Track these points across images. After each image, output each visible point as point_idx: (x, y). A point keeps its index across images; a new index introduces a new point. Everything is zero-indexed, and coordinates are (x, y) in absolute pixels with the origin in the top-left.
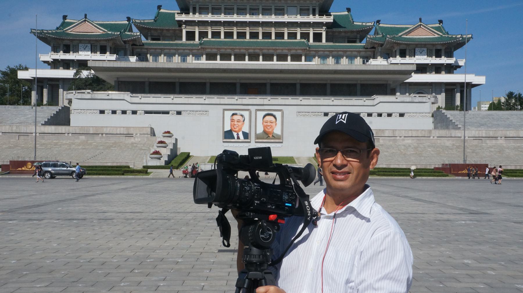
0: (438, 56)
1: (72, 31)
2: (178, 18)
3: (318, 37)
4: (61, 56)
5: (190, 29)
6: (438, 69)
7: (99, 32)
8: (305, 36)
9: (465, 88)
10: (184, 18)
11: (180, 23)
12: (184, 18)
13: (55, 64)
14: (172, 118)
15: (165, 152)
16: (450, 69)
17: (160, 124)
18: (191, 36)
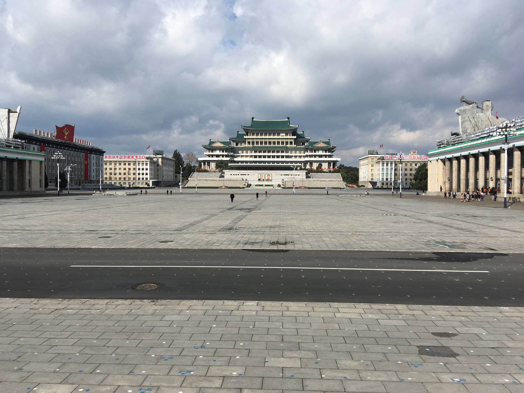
0: (326, 152)
1: (214, 145)
2: (245, 137)
3: (291, 143)
4: (211, 153)
5: (249, 140)
6: (326, 156)
7: (222, 145)
8: (287, 143)
9: (335, 163)
10: (246, 137)
11: (246, 139)
12: (246, 137)
13: (209, 156)
14: (247, 176)
15: (246, 184)
16: (330, 156)
17: (245, 177)
18: (249, 143)
